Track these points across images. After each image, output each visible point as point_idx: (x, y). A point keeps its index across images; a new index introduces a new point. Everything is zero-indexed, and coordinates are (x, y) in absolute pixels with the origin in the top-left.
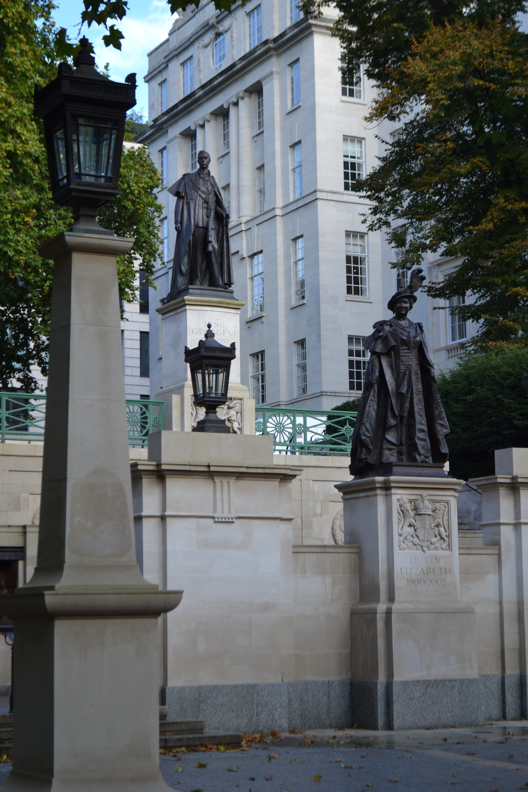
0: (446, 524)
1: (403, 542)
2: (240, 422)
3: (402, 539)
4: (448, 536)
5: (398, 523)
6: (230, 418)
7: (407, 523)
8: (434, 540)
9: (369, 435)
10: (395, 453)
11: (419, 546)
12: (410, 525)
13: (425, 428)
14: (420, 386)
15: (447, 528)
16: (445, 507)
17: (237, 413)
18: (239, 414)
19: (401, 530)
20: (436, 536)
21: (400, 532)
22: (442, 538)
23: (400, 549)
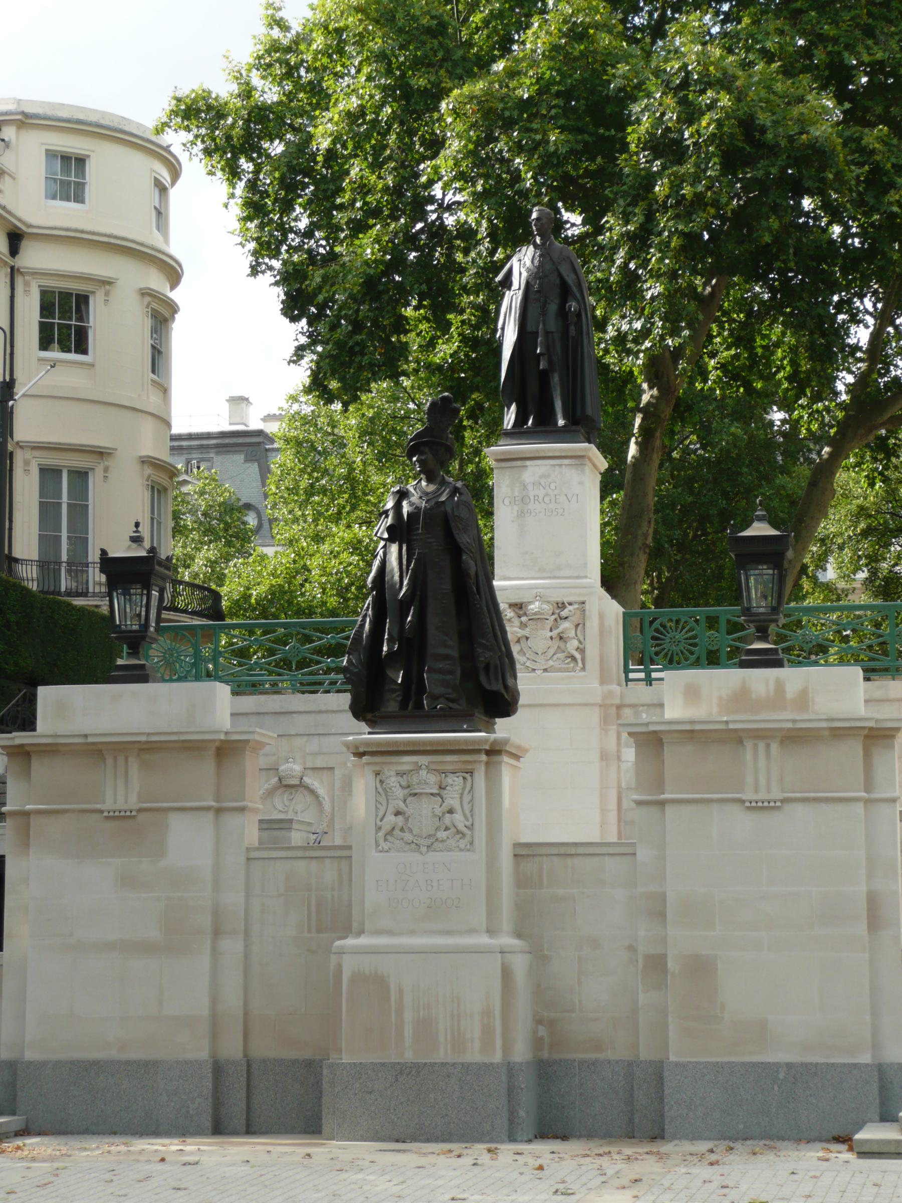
0: (467, 808)
1: (386, 840)
2: (581, 639)
3: (381, 834)
4: (471, 828)
5: (376, 807)
6: (564, 636)
7: (391, 809)
8: (442, 834)
9: (356, 670)
10: (398, 696)
11: (413, 846)
12: (398, 813)
13: (455, 653)
14: (447, 586)
16: (464, 778)
17: (577, 626)
18: (581, 626)
19: (381, 820)
20: (447, 829)
21: (379, 823)
22: (458, 832)
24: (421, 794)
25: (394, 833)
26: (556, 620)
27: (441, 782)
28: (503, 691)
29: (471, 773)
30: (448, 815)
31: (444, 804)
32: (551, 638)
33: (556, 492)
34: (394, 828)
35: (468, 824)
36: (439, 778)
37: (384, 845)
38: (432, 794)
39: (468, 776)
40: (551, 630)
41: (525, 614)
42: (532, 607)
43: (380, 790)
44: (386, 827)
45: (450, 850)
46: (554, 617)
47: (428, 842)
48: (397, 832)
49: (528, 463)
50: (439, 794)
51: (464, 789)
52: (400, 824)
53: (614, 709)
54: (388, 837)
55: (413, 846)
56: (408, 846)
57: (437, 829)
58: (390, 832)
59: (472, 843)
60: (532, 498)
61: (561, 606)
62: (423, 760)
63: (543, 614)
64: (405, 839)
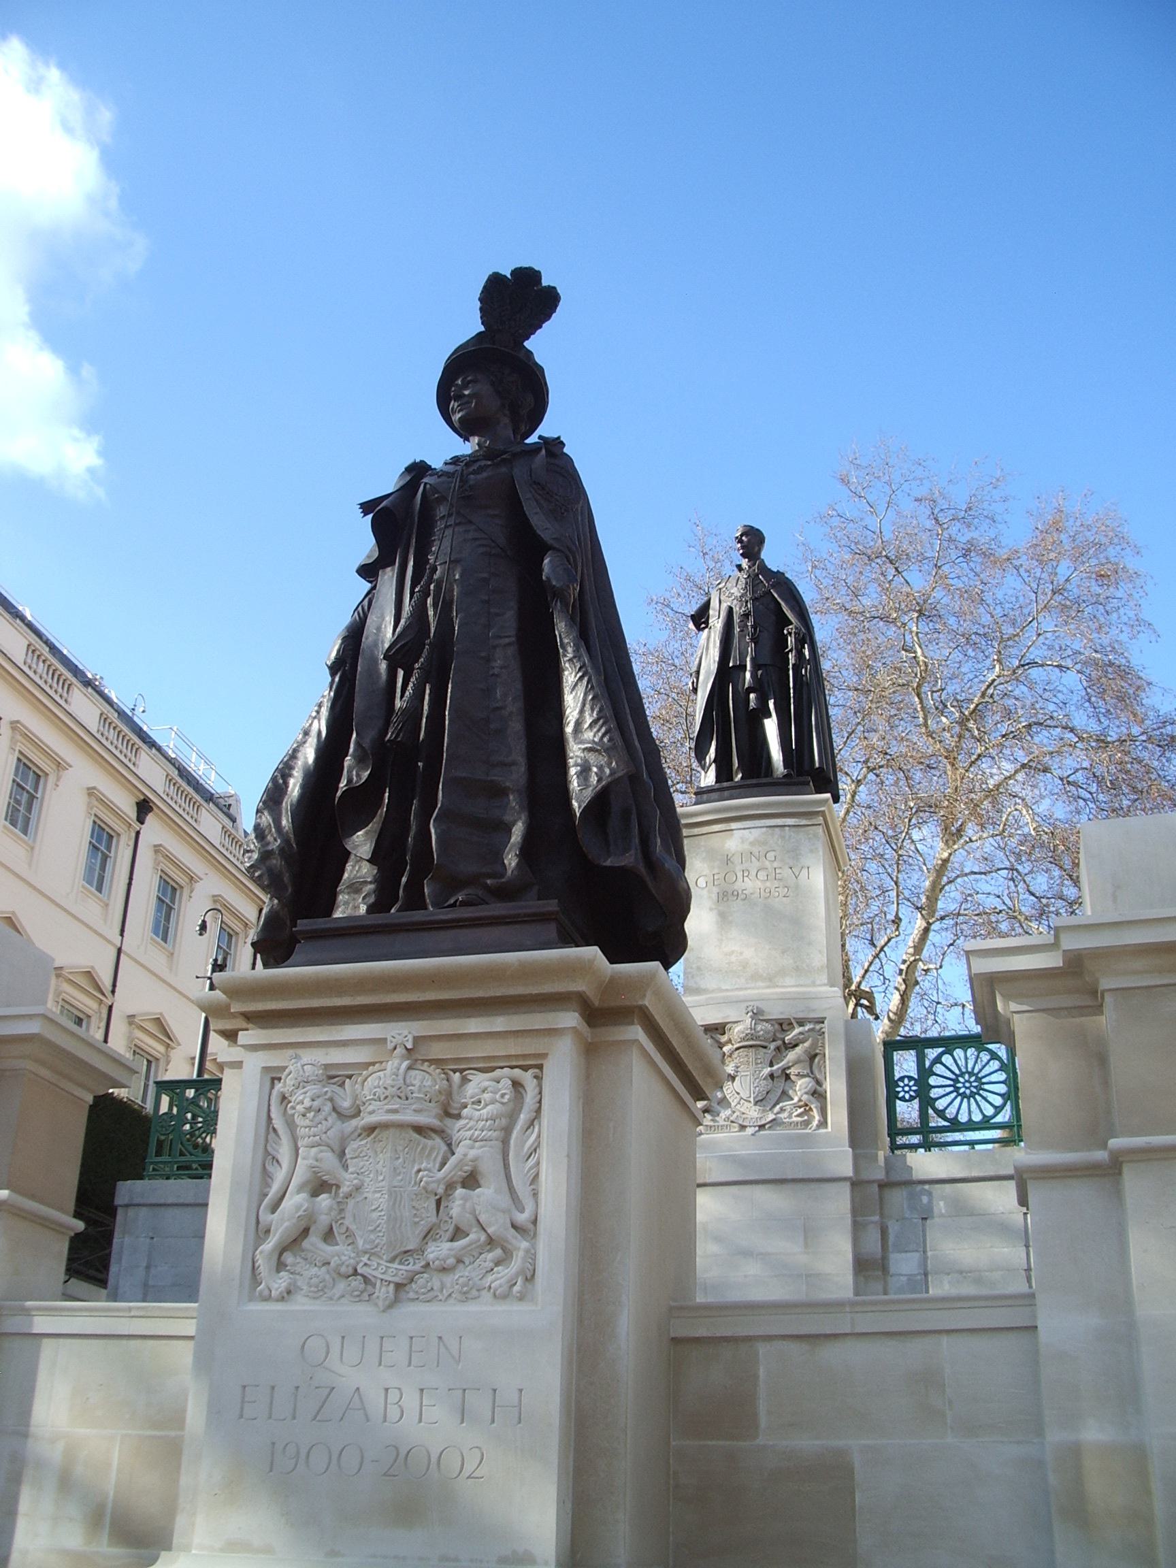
1: (280, 1266)
3: (269, 1245)
15: (523, 1190)
16: (516, 1084)
20: (458, 1234)
22: (491, 1242)
23: (267, 1298)
24: (385, 1126)
25: (306, 1244)
26: (778, 1048)
27: (449, 1094)
28: (642, 870)
29: (536, 1066)
30: (460, 1191)
31: (453, 1160)
32: (772, 1076)
33: (776, 865)
34: (305, 1232)
35: (522, 1218)
36: (441, 1084)
37: (280, 1282)
38: (419, 1129)
39: (527, 1078)
40: (771, 1065)
41: (730, 1041)
42: (738, 1028)
43: (278, 1123)
44: (282, 1223)
45: (466, 1296)
46: (772, 1046)
47: (398, 1271)
48: (313, 1241)
49: (734, 825)
50: (440, 1132)
51: (512, 1117)
52: (324, 1220)
53: (875, 1188)
54: (289, 1258)
55: (357, 1283)
56: (342, 1286)
57: (429, 1234)
58: (295, 1242)
59: (530, 1278)
60: (740, 875)
61: (784, 1025)
62: (401, 1032)
63: (757, 1038)
64: (334, 1262)
